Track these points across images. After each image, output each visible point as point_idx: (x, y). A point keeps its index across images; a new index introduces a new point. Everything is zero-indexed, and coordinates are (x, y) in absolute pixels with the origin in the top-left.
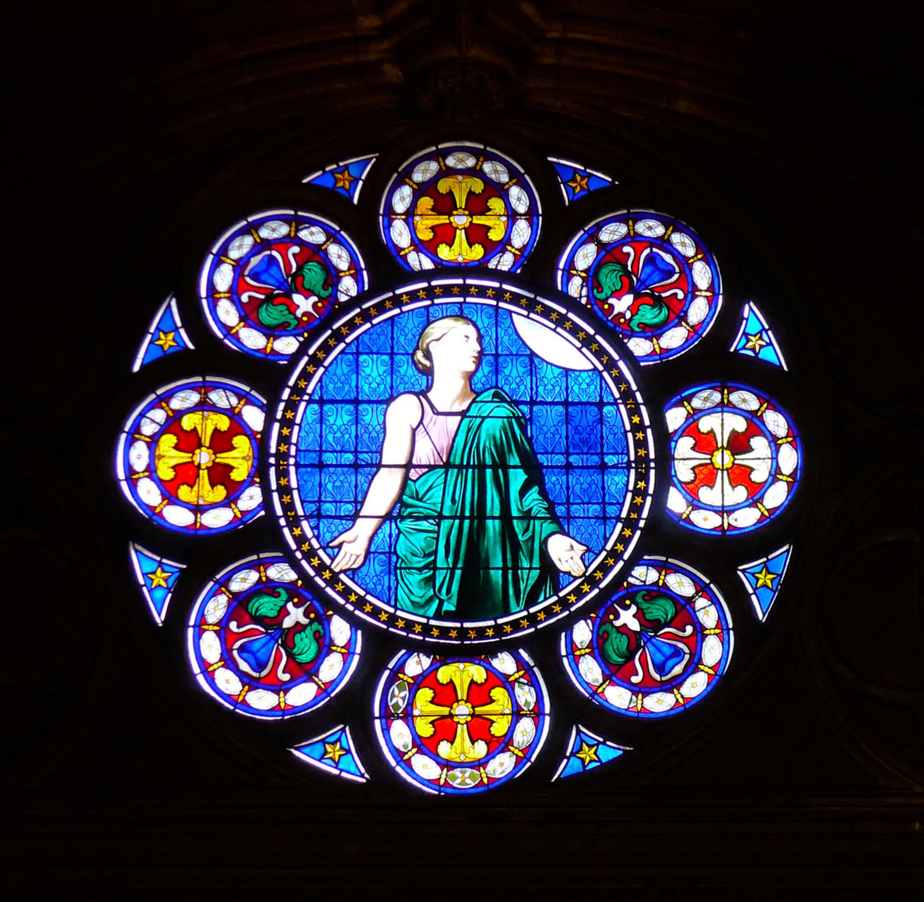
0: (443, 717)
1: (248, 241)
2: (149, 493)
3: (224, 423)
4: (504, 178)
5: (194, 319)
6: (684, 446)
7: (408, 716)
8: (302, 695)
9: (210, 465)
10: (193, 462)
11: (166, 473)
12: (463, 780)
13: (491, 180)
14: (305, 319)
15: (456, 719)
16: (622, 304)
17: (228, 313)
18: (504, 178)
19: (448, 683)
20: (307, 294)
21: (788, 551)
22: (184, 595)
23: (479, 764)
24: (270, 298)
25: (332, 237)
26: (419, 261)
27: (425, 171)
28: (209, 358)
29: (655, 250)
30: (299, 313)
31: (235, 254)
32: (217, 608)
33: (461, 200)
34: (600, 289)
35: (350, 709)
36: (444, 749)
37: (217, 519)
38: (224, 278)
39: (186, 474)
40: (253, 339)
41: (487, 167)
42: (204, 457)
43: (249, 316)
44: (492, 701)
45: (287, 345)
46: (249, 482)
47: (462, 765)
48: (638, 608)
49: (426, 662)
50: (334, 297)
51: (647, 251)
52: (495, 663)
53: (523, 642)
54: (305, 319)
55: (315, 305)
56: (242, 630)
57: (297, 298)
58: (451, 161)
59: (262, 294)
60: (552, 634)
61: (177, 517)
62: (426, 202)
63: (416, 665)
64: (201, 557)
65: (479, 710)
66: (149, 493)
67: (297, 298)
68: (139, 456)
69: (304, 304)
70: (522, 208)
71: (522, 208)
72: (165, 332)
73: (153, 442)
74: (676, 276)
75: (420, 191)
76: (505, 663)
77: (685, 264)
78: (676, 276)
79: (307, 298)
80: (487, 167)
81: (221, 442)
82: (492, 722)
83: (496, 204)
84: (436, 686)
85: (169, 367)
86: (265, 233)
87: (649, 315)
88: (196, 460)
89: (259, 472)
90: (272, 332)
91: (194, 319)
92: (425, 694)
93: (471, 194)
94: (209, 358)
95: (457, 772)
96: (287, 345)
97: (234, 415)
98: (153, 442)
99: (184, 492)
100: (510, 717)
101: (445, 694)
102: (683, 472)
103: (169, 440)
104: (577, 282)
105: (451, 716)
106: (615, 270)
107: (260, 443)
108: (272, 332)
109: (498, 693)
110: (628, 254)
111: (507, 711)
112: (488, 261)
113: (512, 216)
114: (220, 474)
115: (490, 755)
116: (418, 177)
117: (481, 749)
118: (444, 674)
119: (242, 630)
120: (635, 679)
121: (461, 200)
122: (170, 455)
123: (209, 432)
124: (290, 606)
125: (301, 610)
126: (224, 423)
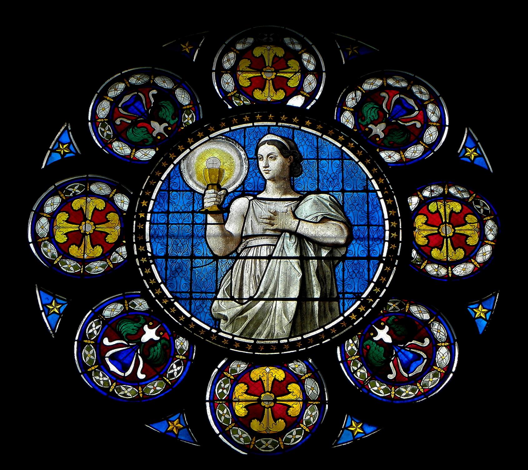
1: (121, 86)
2: (50, 250)
9: (92, 232)
10: (80, 230)
11: (61, 238)
12: (267, 446)
13: (289, 48)
14: (159, 138)
16: (379, 130)
18: (298, 47)
22: (70, 320)
24: (134, 124)
25: (178, 84)
30: (154, 134)
31: (112, 94)
33: (269, 61)
37: (97, 268)
38: (104, 109)
39: (76, 238)
42: (88, 228)
46: (118, 244)
49: (244, 366)
51: (398, 96)
54: (159, 138)
55: (165, 129)
59: (130, 120)
61: (69, 267)
62: (245, 64)
66: (50, 250)
67: (154, 124)
69: (158, 128)
70: (311, 67)
71: (311, 67)
72: (63, 145)
73: (52, 218)
74: (416, 113)
75: (240, 55)
76: (298, 367)
77: (422, 106)
78: (416, 113)
81: (100, 217)
83: (293, 64)
85: (64, 168)
86: (133, 80)
88: (82, 228)
89: (125, 236)
91: (82, 136)
92: (241, 388)
94: (92, 163)
96: (146, 155)
97: (109, 200)
98: (52, 218)
100: (301, 403)
101: (255, 388)
103: (62, 217)
104: (347, 114)
106: (373, 108)
107: (126, 219)
108: (136, 146)
109: (294, 388)
113: (304, 72)
114: (98, 238)
115: (287, 429)
116: (239, 47)
117: (281, 424)
118: (256, 374)
120: (391, 377)
121: (269, 61)
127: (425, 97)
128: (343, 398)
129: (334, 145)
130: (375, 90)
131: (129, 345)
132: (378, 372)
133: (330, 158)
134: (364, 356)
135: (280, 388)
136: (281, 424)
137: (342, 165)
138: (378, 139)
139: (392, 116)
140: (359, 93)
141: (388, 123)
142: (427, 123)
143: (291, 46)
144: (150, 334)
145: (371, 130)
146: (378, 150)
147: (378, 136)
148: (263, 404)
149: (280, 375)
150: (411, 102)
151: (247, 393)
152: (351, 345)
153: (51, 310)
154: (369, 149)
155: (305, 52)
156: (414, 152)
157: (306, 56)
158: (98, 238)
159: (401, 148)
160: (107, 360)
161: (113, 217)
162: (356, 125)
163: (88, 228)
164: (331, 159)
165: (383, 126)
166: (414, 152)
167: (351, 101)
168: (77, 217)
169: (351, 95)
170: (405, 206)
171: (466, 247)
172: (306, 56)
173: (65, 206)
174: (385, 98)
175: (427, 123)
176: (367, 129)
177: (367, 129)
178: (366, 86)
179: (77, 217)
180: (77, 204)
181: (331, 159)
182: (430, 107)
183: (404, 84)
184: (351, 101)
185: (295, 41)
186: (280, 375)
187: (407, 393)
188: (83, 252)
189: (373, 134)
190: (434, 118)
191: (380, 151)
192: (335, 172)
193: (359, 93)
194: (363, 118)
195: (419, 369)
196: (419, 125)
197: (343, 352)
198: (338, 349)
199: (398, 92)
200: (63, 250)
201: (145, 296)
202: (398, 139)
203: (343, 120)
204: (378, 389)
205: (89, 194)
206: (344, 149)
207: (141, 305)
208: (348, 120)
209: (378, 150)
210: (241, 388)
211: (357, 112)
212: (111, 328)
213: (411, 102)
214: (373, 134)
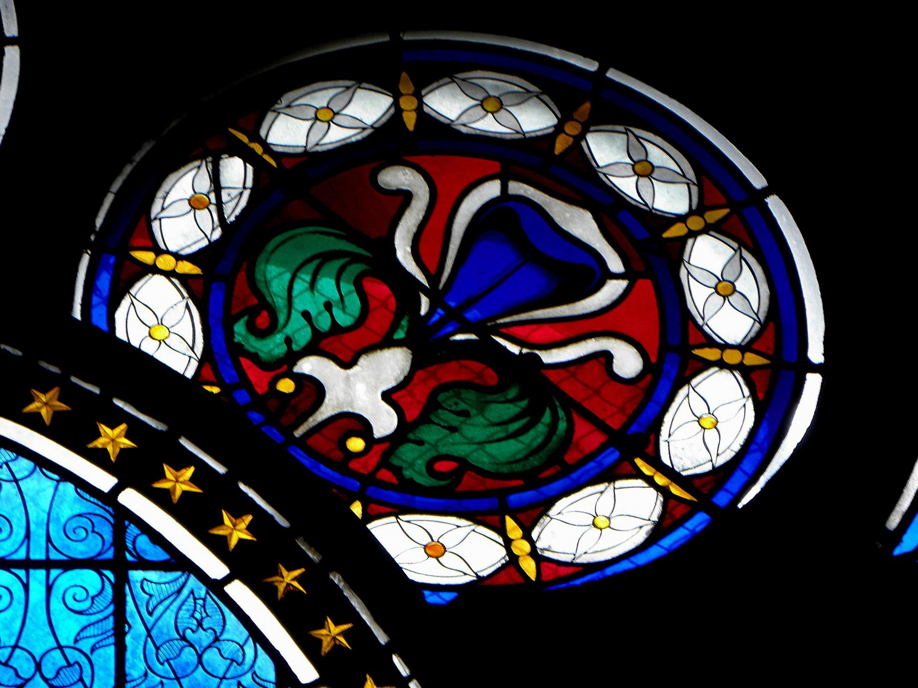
16: (363, 389)
34: (265, 319)
51: (491, 190)
74: (612, 290)
77: (653, 247)
78: (612, 290)
110: (405, 198)
127: (671, 199)
129: (66, 475)
130: (345, 150)
133: (38, 554)
137: (119, 601)
138: (356, 444)
139: (455, 303)
140: (235, 171)
141: (426, 348)
142: (679, 351)
145: (313, 390)
146: (357, 509)
147: (358, 424)
150: (582, 225)
154: (296, 504)
156: (601, 524)
159: (508, 498)
164: (47, 564)
165: (392, 365)
166: (601, 524)
167: (182, 220)
169: (187, 183)
175: (679, 351)
176: (286, 386)
177: (286, 386)
178: (287, 132)
181: (47, 564)
182: (708, 255)
183: (535, 119)
184: (182, 220)
189: (326, 411)
190: (731, 324)
191: (369, 516)
192: (66, 638)
193: (235, 171)
194: (263, 320)
196: (627, 362)
199: (496, 167)
202: (488, 438)
206: (131, 499)
208: (160, 322)
209: (357, 509)
211: (220, 281)
213: (582, 225)
214: (326, 411)
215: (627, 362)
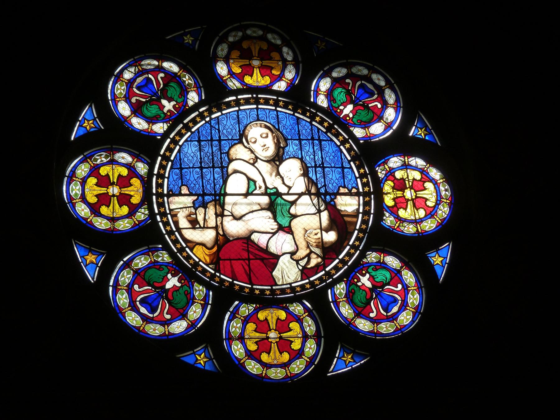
0: (263, 339)
3: (124, 172)
4: (279, 42)
5: (106, 112)
6: (388, 187)
7: (241, 338)
8: (179, 327)
11: (92, 200)
13: (272, 43)
15: (270, 340)
17: (124, 109)
18: (279, 42)
19: (264, 320)
20: (170, 100)
21: (449, 245)
23: (284, 366)
26: (234, 84)
27: (235, 36)
28: (115, 135)
29: (363, 82)
32: (126, 277)
33: (255, 52)
35: (209, 334)
36: (264, 357)
37: (124, 225)
39: (104, 199)
40: (139, 124)
41: (269, 36)
43: (137, 110)
44: (290, 330)
45: (159, 128)
47: (276, 366)
48: (370, 275)
50: (185, 102)
52: (291, 309)
53: (307, 297)
55: (174, 107)
56: (141, 290)
57: (164, 102)
58: (249, 32)
60: (324, 291)
61: (101, 224)
63: (245, 310)
64: (114, 246)
65: (284, 335)
67: (164, 102)
68: (76, 189)
69: (168, 106)
70: (289, 58)
71: (289, 58)
72: (87, 120)
73: (84, 182)
75: (232, 47)
76: (297, 309)
77: (381, 91)
79: (169, 102)
80: (269, 36)
81: (123, 182)
82: (292, 342)
84: (257, 322)
87: (364, 115)
90: (152, 120)
92: (251, 327)
93: (260, 49)
94: (115, 135)
95: (273, 370)
99: (104, 210)
101: (263, 327)
102: (389, 201)
105: (268, 338)
106: (342, 92)
108: (152, 120)
109: (294, 325)
111: (300, 336)
112: (272, 86)
114: (124, 199)
116: (231, 39)
117: (286, 357)
118: (261, 316)
119: (141, 290)
121: (255, 52)
122: (93, 191)
123: (116, 176)
124: (169, 276)
125: (176, 278)
126: (124, 172)
127: (383, 83)
128: (334, 334)
131: (155, 291)
132: (361, 312)
134: (350, 297)
135: (282, 326)
136: (286, 357)
138: (348, 118)
143: (273, 41)
144: (172, 282)
148: (270, 340)
149: (283, 315)
151: (255, 331)
152: (341, 289)
153: (90, 263)
155: (284, 46)
157: (285, 49)
158: (124, 199)
160: (138, 303)
161: (136, 182)
162: (330, 105)
163: (115, 190)
168: (104, 181)
170: (374, 174)
171: (426, 207)
172: (285, 49)
173: (94, 171)
174: (349, 83)
179: (104, 181)
180: (103, 171)
185: (276, 37)
186: (283, 315)
187: (386, 328)
188: (112, 211)
195: (395, 309)
197: (334, 295)
198: (329, 291)
200: (95, 209)
201: (166, 248)
203: (319, 103)
204: (363, 325)
205: (113, 162)
207: (165, 257)
210: (251, 327)
212: (140, 276)
215: (379, 106)
